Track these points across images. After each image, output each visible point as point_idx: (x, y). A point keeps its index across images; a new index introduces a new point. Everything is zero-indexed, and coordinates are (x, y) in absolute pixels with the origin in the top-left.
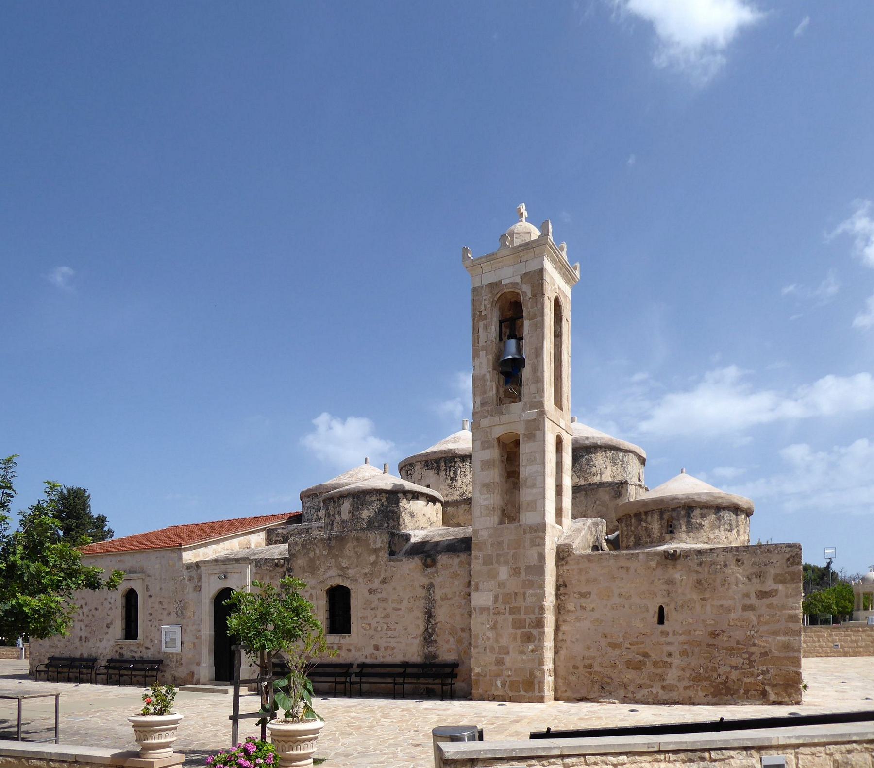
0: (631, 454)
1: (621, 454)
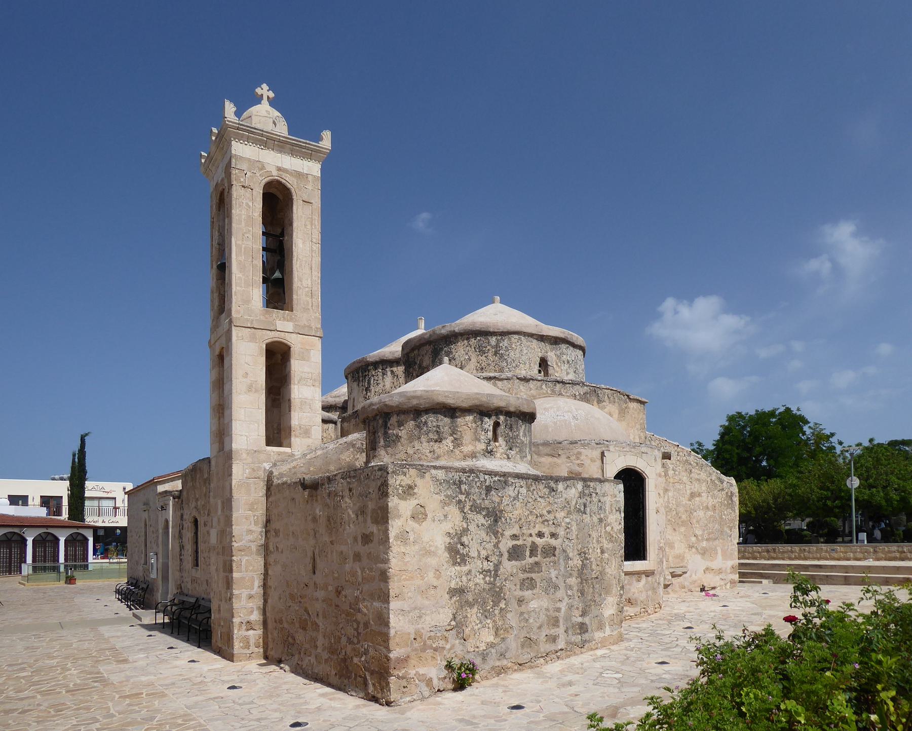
0: (516, 336)
1: (493, 340)
